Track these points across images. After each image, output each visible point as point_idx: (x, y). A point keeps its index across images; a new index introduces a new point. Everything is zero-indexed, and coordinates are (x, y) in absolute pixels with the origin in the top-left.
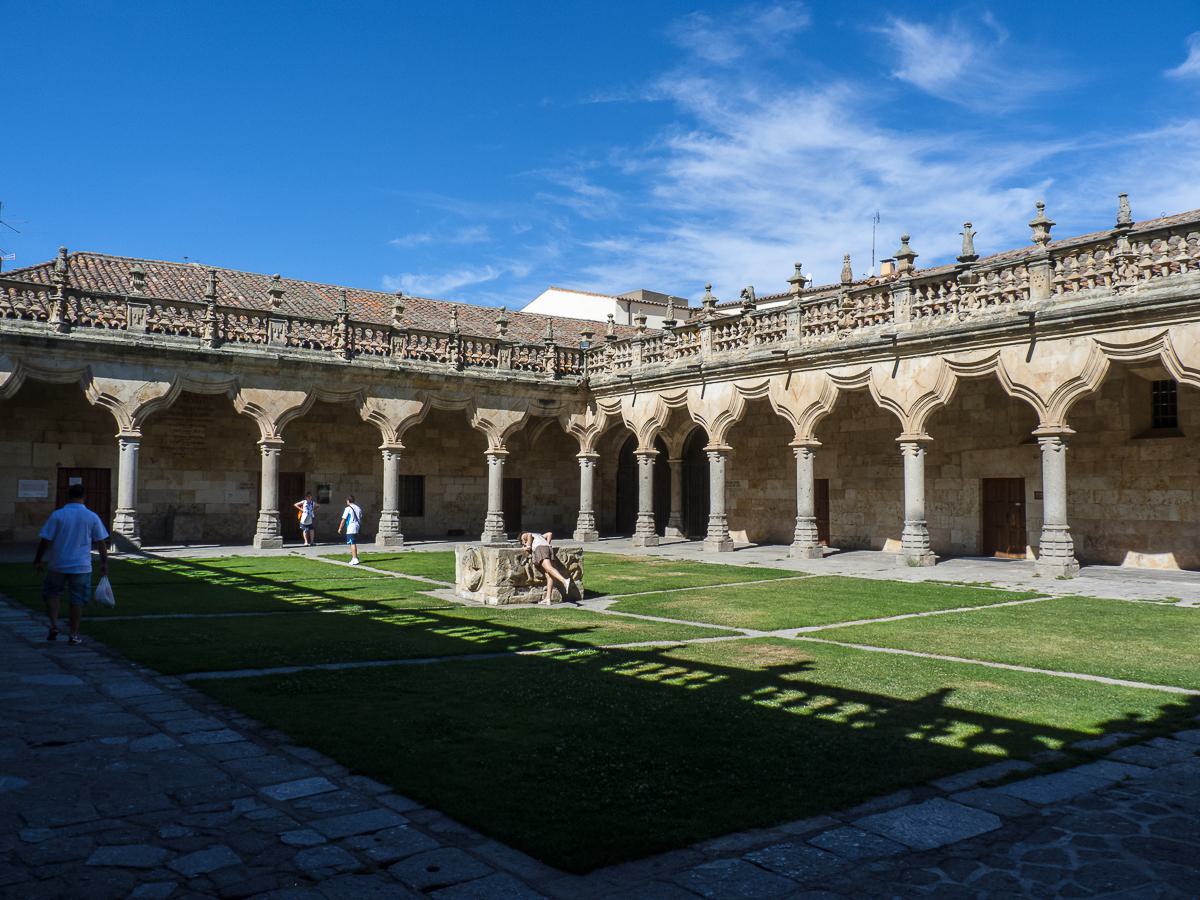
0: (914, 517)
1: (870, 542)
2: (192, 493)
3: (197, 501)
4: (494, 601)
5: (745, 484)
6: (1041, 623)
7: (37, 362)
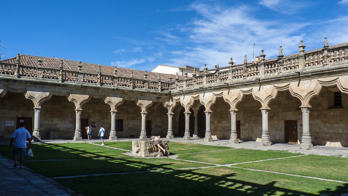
0: (265, 132)
2: (56, 125)
3: (57, 127)
4: (143, 156)
5: (216, 122)
6: (302, 162)
7: (11, 86)
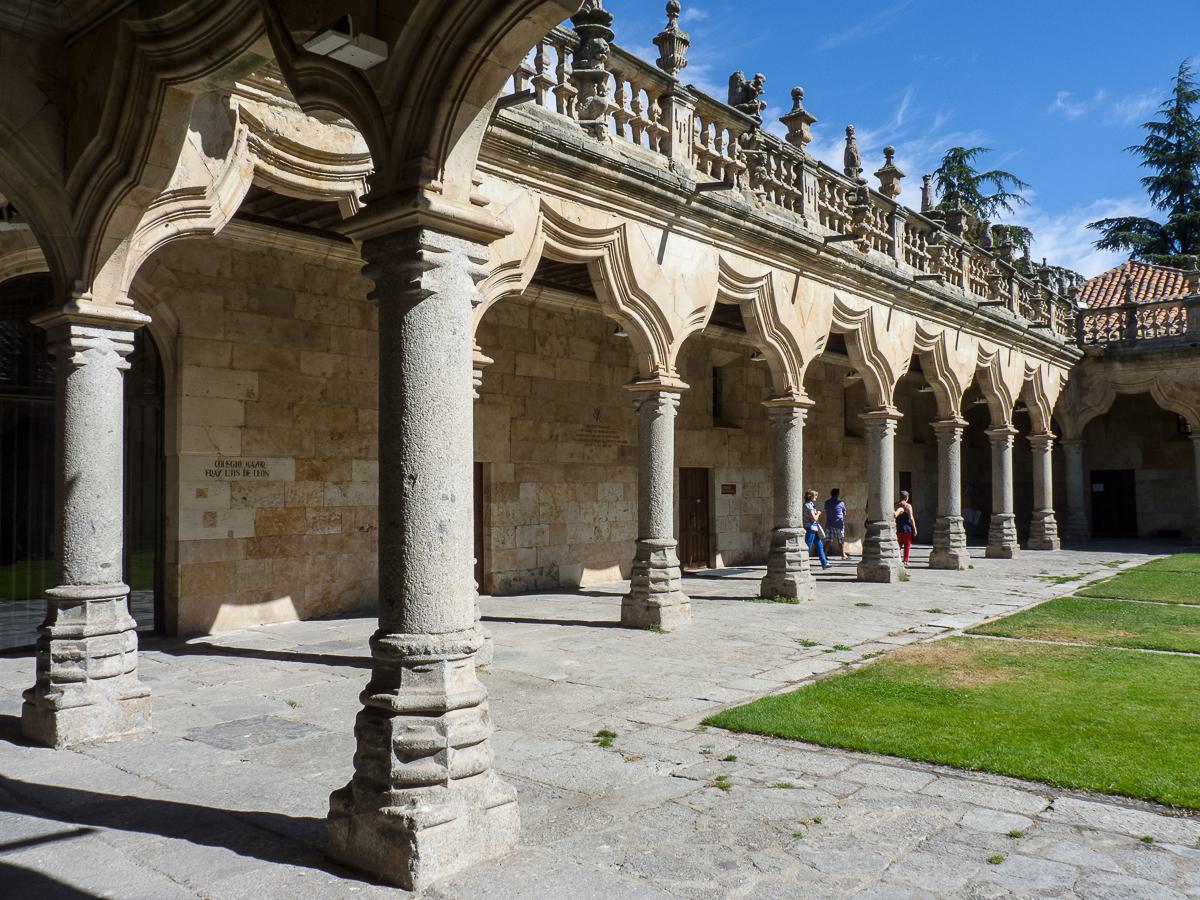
1: (557, 572)
